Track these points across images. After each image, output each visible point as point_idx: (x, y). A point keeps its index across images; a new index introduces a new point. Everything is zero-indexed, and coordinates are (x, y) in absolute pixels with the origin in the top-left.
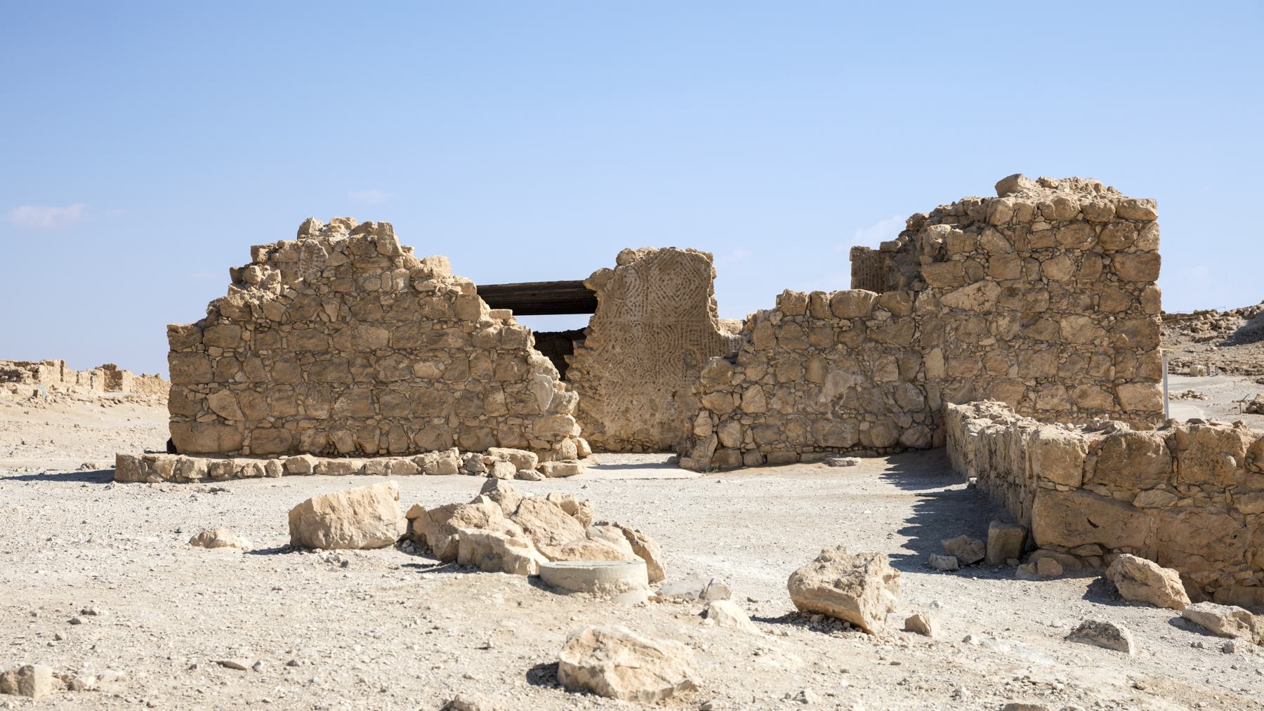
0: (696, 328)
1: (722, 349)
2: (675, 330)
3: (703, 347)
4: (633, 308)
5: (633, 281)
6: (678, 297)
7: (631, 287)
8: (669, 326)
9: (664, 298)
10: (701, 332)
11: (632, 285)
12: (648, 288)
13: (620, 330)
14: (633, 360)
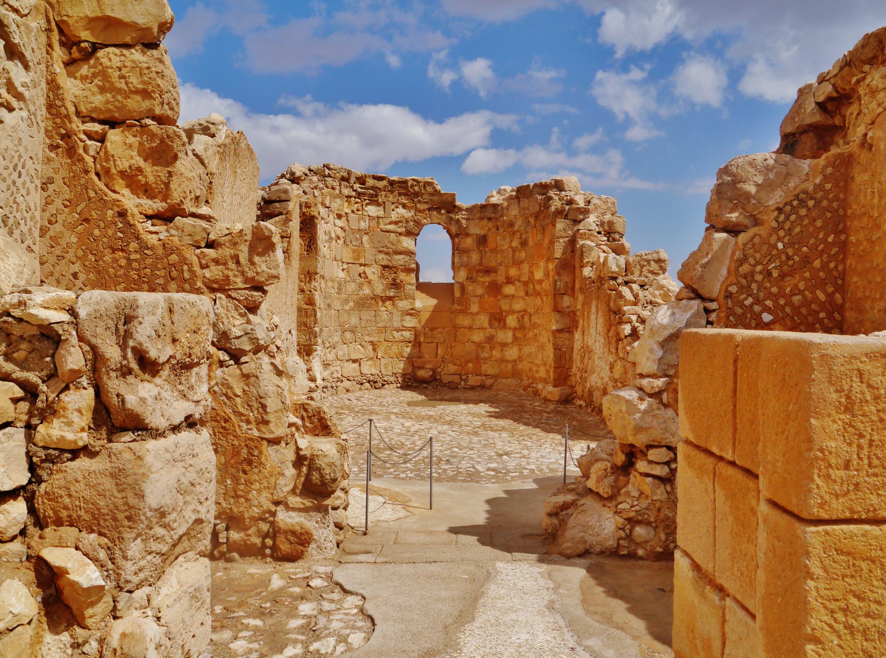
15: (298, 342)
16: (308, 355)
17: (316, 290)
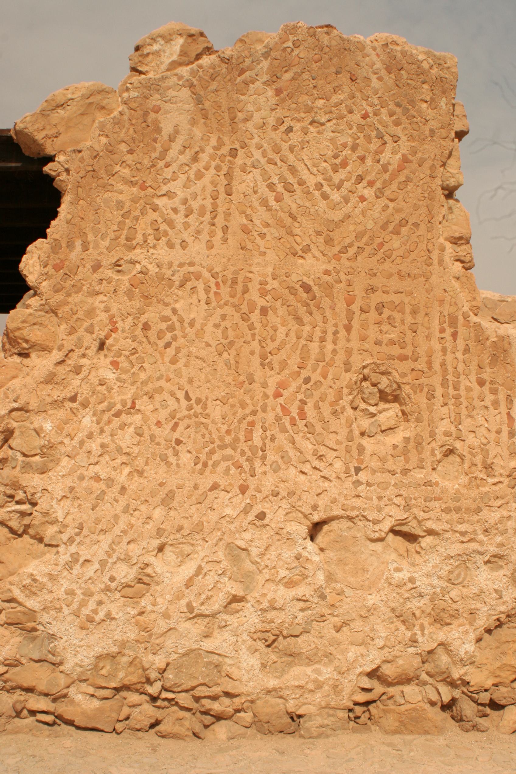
0: (397, 299)
1: (484, 376)
2: (326, 303)
3: (421, 365)
4: (179, 219)
5: (185, 126)
6: (339, 188)
7: (176, 146)
10: (414, 312)
11: (180, 140)
12: (233, 153)
13: (130, 294)
14: (172, 403)
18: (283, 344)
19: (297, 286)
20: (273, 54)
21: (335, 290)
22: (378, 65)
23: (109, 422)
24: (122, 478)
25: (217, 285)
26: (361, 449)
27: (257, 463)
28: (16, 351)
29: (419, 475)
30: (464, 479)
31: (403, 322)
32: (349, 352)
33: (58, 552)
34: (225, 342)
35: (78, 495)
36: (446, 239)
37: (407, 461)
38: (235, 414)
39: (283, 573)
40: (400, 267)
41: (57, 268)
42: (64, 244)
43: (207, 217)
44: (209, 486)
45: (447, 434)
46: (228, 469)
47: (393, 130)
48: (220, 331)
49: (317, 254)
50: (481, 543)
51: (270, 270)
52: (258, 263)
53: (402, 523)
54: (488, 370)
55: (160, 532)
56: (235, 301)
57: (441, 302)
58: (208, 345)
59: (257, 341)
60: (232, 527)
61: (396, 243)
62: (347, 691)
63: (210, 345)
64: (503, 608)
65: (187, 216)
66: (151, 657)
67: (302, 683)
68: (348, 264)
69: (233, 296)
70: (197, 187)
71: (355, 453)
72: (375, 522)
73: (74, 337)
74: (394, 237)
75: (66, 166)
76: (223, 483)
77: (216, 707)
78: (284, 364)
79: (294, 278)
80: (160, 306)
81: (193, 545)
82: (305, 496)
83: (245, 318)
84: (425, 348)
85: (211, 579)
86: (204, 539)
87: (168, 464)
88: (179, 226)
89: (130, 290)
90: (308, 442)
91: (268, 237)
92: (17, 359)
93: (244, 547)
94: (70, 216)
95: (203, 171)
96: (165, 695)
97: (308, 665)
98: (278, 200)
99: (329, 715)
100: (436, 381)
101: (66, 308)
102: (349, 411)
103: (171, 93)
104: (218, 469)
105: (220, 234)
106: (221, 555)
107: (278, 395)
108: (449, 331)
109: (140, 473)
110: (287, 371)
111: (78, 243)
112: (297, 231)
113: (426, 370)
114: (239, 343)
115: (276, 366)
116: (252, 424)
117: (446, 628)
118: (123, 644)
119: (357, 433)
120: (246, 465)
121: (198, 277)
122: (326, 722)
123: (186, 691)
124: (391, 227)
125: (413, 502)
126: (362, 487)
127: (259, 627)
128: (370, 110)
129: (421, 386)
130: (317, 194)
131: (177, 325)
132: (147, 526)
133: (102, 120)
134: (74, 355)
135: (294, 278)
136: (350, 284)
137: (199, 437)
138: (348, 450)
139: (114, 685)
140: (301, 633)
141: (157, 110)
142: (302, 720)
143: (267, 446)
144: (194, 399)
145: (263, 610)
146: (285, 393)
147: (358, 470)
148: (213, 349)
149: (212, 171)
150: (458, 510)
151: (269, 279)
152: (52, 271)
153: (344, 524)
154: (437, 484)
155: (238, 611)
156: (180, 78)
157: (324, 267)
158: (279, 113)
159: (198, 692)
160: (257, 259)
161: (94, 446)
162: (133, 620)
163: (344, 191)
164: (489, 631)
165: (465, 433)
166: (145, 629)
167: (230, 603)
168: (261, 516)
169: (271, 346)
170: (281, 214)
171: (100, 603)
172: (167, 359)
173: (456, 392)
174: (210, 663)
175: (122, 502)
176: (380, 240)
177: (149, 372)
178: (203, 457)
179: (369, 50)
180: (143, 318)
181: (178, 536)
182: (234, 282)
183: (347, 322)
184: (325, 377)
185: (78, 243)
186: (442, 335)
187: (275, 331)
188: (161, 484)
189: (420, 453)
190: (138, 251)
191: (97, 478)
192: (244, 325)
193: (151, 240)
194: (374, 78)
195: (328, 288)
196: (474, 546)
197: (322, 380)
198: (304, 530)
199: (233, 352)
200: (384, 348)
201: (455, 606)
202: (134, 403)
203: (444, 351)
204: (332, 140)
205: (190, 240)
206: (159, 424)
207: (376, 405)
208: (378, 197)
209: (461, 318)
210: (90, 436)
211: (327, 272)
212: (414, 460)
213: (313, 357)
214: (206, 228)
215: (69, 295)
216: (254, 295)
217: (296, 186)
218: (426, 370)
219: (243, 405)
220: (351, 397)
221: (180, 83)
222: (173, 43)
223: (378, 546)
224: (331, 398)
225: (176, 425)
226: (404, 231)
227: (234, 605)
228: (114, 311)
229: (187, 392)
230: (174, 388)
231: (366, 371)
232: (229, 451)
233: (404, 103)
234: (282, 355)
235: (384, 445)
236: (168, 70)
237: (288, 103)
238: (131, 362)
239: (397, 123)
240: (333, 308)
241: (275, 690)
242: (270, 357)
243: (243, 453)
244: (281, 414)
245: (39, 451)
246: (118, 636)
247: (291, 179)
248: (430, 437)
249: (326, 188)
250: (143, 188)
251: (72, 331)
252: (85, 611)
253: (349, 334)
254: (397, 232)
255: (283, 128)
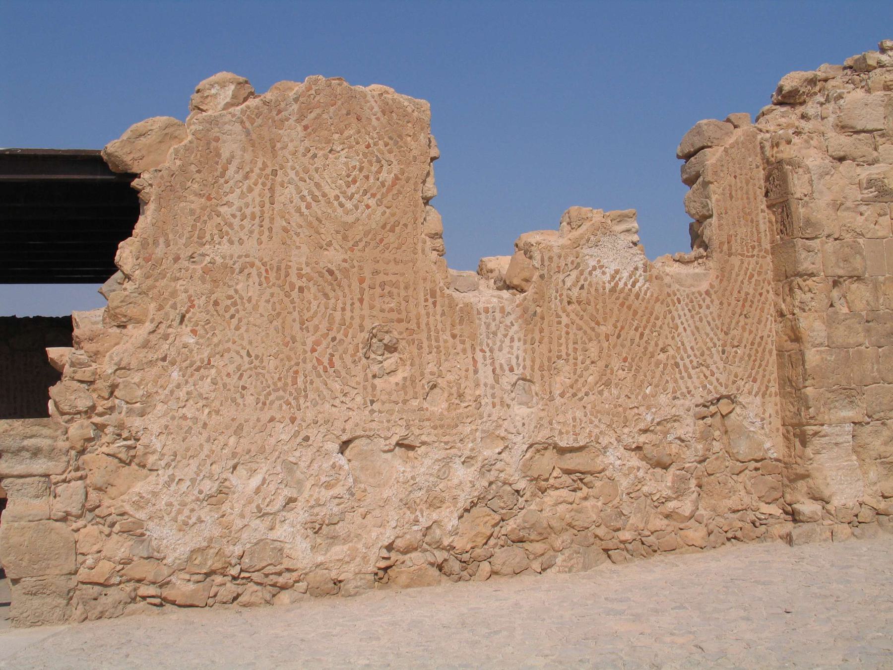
0: (393, 278)
1: (455, 332)
2: (345, 282)
4: (236, 222)
5: (239, 153)
6: (351, 198)
7: (232, 169)
8: (331, 273)
9: (315, 199)
10: (406, 288)
12: (275, 173)
13: (203, 280)
15: (783, 419)
16: (804, 444)
17: (804, 311)
18: (316, 313)
19: (324, 271)
20: (301, 99)
21: (351, 274)
22: (376, 109)
23: (192, 375)
24: (204, 416)
25: (267, 271)
26: (374, 387)
27: (302, 401)
28: (116, 324)
29: (415, 403)
30: (444, 405)
31: (399, 295)
32: (362, 318)
33: (158, 475)
34: (274, 313)
35: (171, 431)
36: (426, 235)
37: (406, 394)
38: (283, 366)
39: (323, 479)
40: (395, 256)
41: (147, 260)
42: (150, 241)
43: (257, 221)
44: (268, 418)
45: (432, 373)
46: (281, 406)
47: (387, 156)
48: (270, 305)
49: (338, 247)
50: (459, 449)
51: (304, 259)
52: (295, 255)
53: (405, 438)
54: (459, 327)
55: (234, 455)
56: (280, 282)
57: (425, 280)
58: (262, 315)
59: (297, 312)
60: (285, 448)
61: (391, 238)
62: (373, 558)
63: (263, 316)
64: (476, 494)
65: (242, 220)
66: (231, 548)
67: (341, 557)
68: (359, 254)
69: (278, 279)
70: (249, 199)
71: (370, 389)
72: (386, 439)
73: (162, 312)
74: (391, 234)
75: (150, 182)
76: (278, 416)
77: (281, 580)
78: (317, 328)
79: (321, 265)
80: (226, 288)
81: (258, 463)
82: (335, 423)
83: (288, 295)
84: (415, 313)
85: (272, 487)
86: (266, 458)
87: (238, 405)
88: (236, 228)
89: (202, 276)
90: (336, 384)
91: (302, 235)
92: (118, 331)
93: (295, 462)
94: (154, 221)
95: (253, 186)
96: (243, 575)
97: (344, 544)
98: (308, 207)
99: (361, 579)
100: (424, 336)
101: (156, 291)
102: (364, 360)
103: (227, 127)
104: (273, 406)
105: (267, 233)
106: (279, 469)
107: (313, 350)
108: (431, 300)
109: (217, 412)
110: (319, 333)
111: (161, 240)
112: (323, 231)
113: (416, 329)
114: (284, 313)
115: (311, 329)
116: (296, 372)
117: (438, 510)
118: (211, 540)
119: (370, 376)
120: (293, 403)
121: (252, 265)
122: (359, 584)
123: (258, 571)
124: (388, 227)
125: (412, 422)
126: (376, 414)
127: (309, 519)
128: (371, 141)
129: (413, 340)
130: (336, 203)
131: (239, 301)
132: (224, 451)
133: (176, 147)
134: (163, 326)
135: (321, 265)
136: (361, 268)
137: (259, 383)
138: (365, 388)
139: (205, 571)
140: (338, 522)
141: (217, 140)
142: (342, 584)
143: (308, 388)
144: (253, 356)
145: (312, 507)
146: (318, 348)
147: (372, 402)
148: (265, 318)
149: (260, 186)
150: (442, 426)
151: (304, 266)
152: (143, 263)
153: (364, 441)
154: (427, 409)
155: (292, 509)
156: (234, 115)
157: (343, 257)
158: (307, 143)
159: (266, 571)
160: (295, 252)
161: (182, 394)
162: (218, 521)
163: (354, 201)
164: (467, 510)
165: (444, 372)
166: (226, 527)
167: (287, 504)
168: (307, 439)
169: (307, 315)
170: (310, 218)
171: (193, 510)
172: (232, 327)
173: (437, 344)
174: (275, 548)
175: (205, 435)
176: (381, 236)
177: (219, 337)
178: (262, 398)
179: (369, 97)
180: (213, 297)
181: (247, 456)
182: (279, 269)
183: (360, 296)
184: (346, 336)
185: (161, 240)
186: (426, 304)
187: (310, 304)
188: (233, 420)
189: (415, 388)
190: (207, 246)
191: (184, 417)
192: (286, 300)
193: (216, 238)
194: (373, 118)
195: (345, 272)
196: (453, 451)
197: (345, 339)
198: (336, 447)
199: (280, 320)
200: (386, 314)
201: (444, 494)
202: (209, 360)
203: (428, 314)
204: (346, 164)
205: (245, 238)
206: (228, 375)
207: (383, 355)
208: (378, 205)
209: (438, 290)
210: (178, 386)
211: (345, 261)
212: (411, 393)
213: (337, 322)
214: (256, 229)
215: (157, 281)
216: (293, 278)
217: (320, 198)
218: (416, 329)
219: (289, 359)
220: (365, 350)
221: (234, 119)
222: (227, 88)
223: (389, 455)
224: (351, 351)
225: (241, 376)
226: (397, 229)
227: (292, 505)
228: (191, 292)
229: (248, 351)
230: (239, 348)
231: (374, 331)
232: (281, 393)
233: (395, 137)
234: (316, 321)
235: (390, 383)
236: (224, 109)
237: (313, 135)
238: (206, 330)
239: (390, 152)
240: (349, 286)
241: (321, 564)
242: (307, 323)
243: (291, 394)
244: (316, 364)
245: (139, 400)
246: (207, 534)
247: (317, 193)
248: (421, 376)
249: (342, 199)
250: (209, 198)
251: (160, 308)
252: (181, 518)
253: (362, 305)
254: (392, 230)
255: (309, 155)
